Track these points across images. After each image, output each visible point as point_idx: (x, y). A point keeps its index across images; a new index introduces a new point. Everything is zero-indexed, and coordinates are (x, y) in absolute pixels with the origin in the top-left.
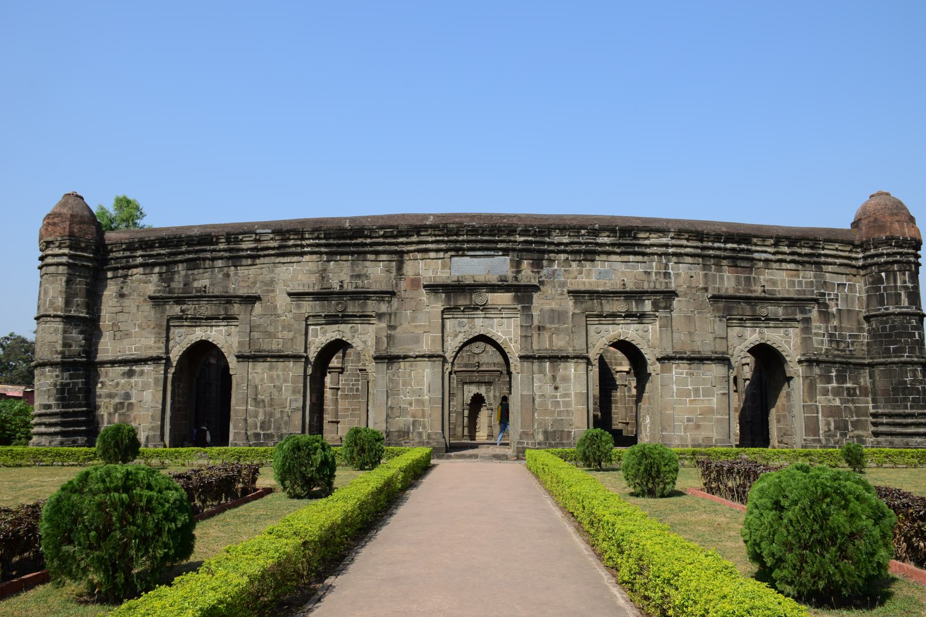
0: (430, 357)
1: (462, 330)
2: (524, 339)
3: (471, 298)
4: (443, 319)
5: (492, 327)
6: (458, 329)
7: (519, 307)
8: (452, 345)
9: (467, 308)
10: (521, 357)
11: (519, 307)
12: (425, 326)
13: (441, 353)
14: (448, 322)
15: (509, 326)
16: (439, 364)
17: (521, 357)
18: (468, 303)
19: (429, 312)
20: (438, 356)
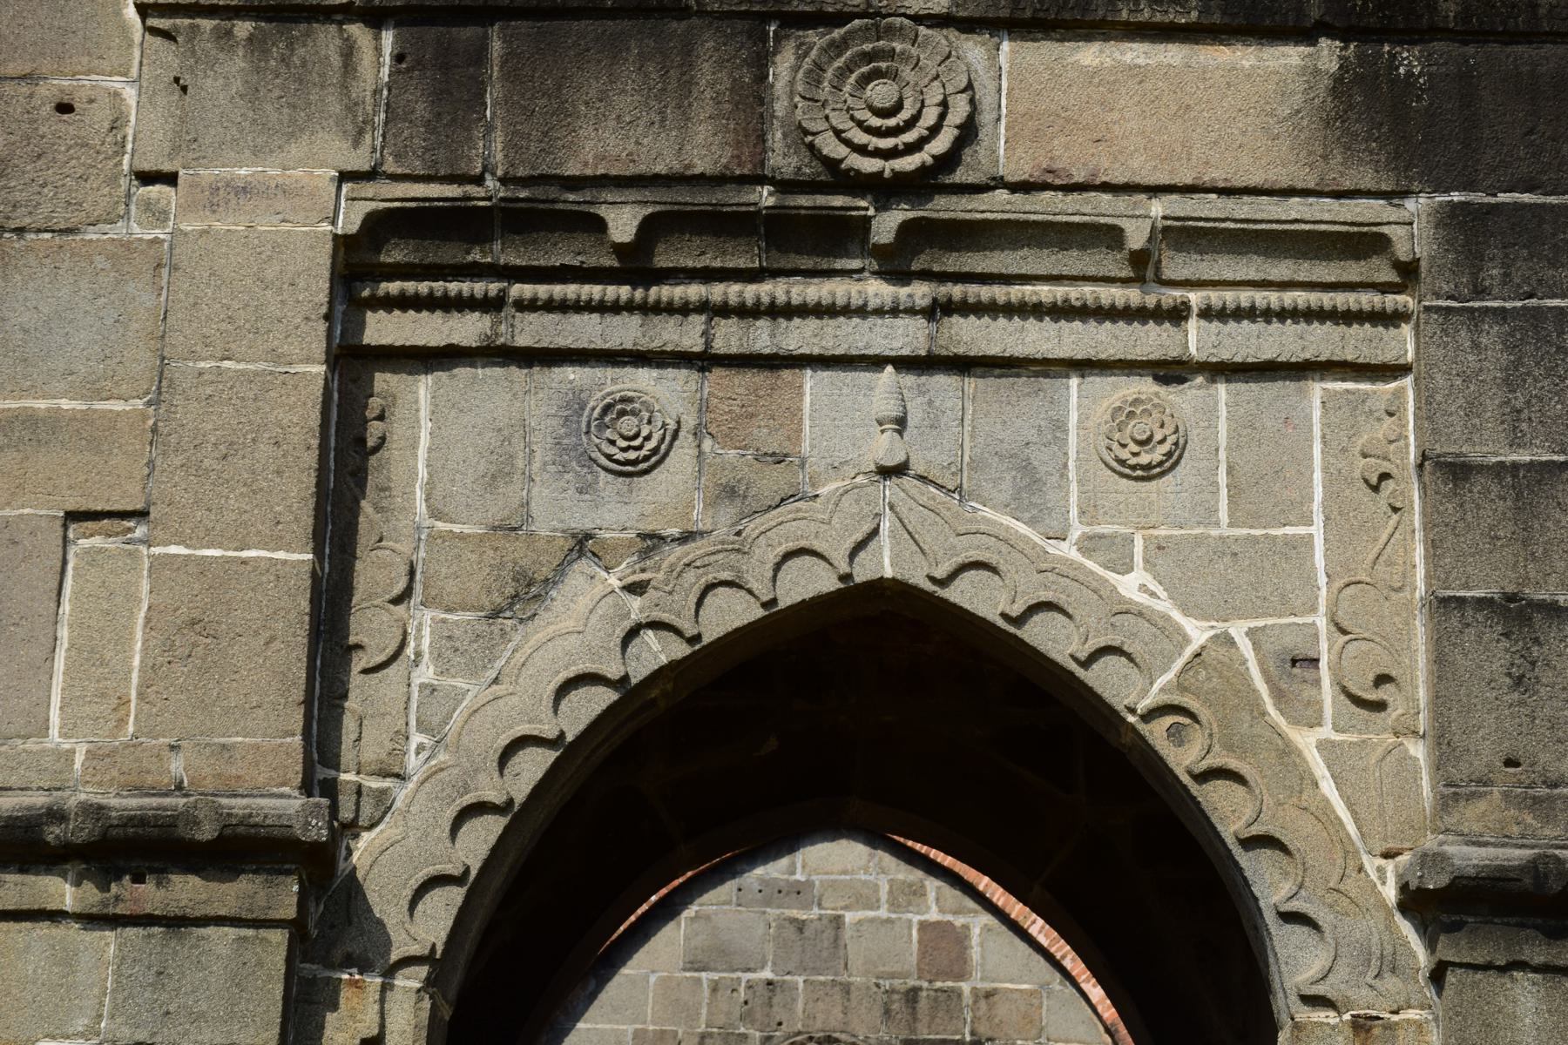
0: (128, 851)
1: (617, 512)
2: (1490, 654)
3: (752, 98)
4: (352, 363)
5: (1031, 487)
6: (556, 508)
7: (1412, 222)
8: (459, 727)
9: (702, 225)
10: (1438, 905)
11: (1412, 222)
12: (91, 434)
13: (285, 805)
14: (418, 410)
15: (1263, 488)
16: (235, 971)
17: (1438, 905)
18: (703, 147)
19: (162, 262)
20: (240, 849)
